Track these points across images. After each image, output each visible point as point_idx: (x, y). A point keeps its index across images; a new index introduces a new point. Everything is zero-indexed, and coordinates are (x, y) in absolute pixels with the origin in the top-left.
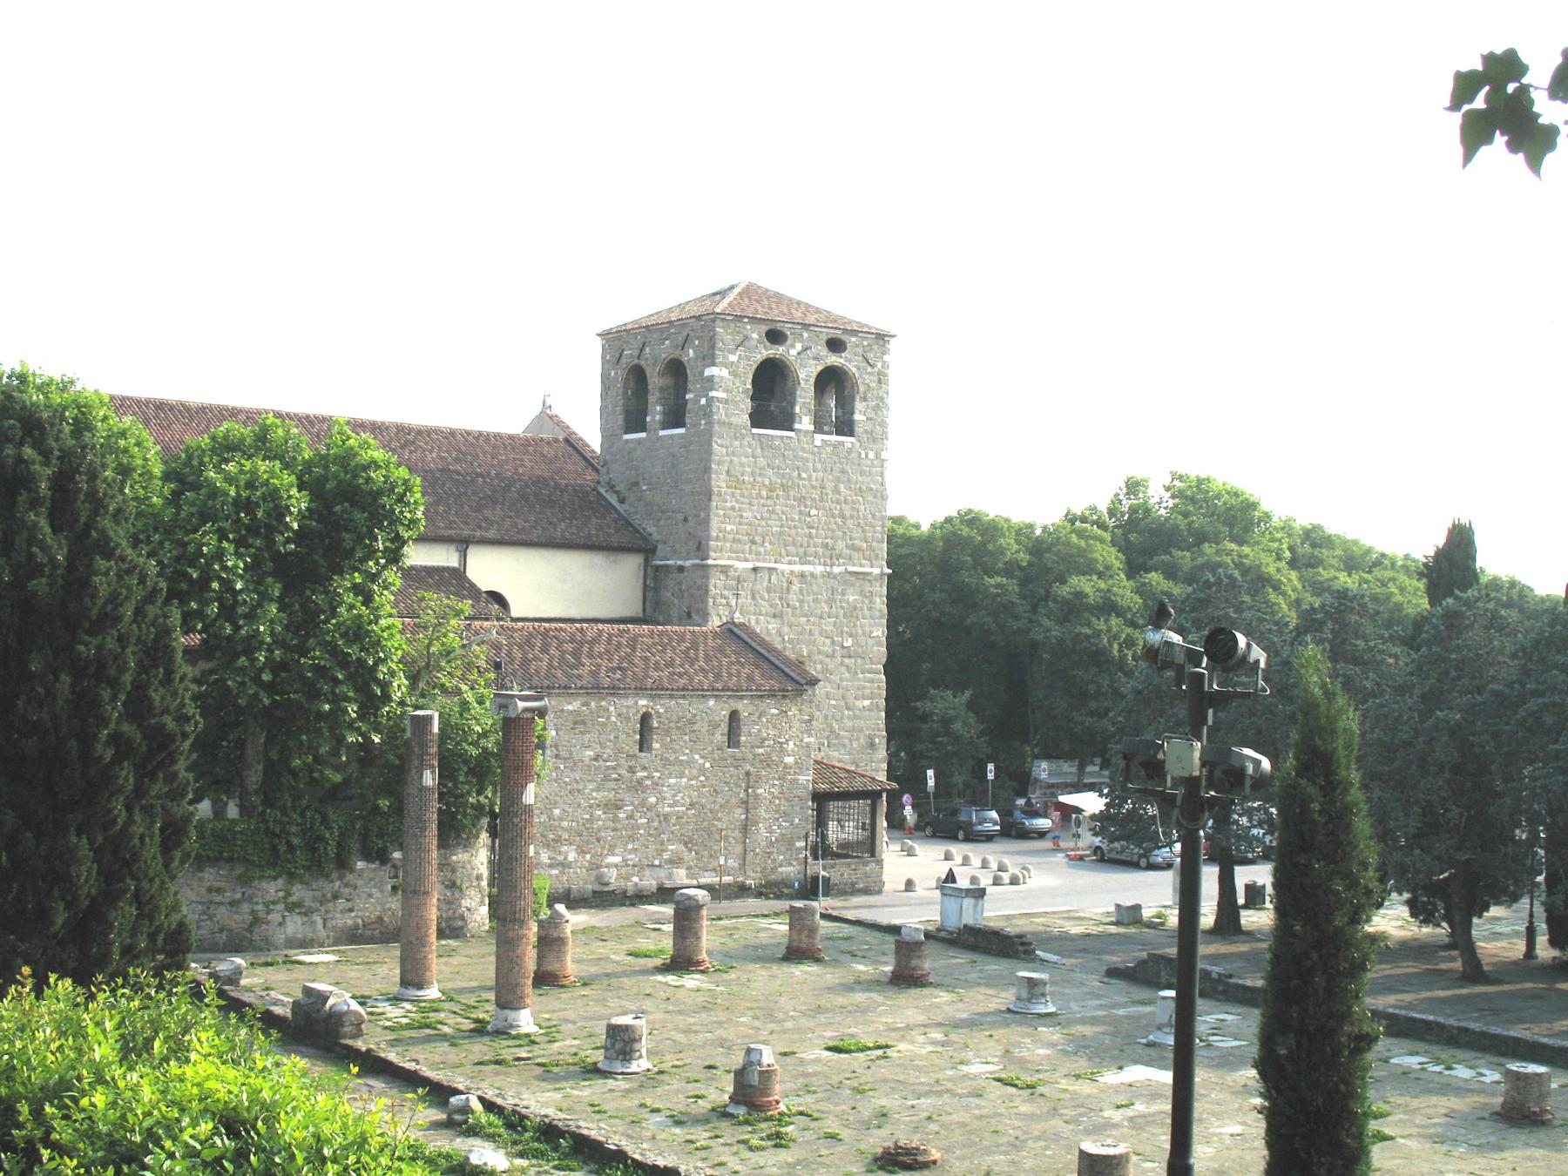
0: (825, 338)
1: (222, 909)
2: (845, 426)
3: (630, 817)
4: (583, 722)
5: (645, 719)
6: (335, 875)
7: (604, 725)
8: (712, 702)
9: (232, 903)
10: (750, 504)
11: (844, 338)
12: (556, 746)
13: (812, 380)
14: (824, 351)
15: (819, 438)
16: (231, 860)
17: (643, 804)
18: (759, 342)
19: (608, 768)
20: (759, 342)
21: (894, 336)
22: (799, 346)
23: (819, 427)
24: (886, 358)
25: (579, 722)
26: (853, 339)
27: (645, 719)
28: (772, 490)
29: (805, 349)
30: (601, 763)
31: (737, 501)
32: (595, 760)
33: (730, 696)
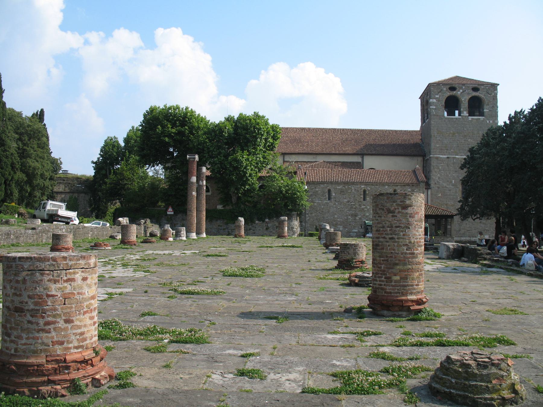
0: (471, 88)
1: (221, 230)
2: (482, 114)
3: (360, 219)
4: (343, 192)
5: (365, 191)
6: (250, 224)
7: (350, 192)
8: (386, 187)
9: (224, 229)
10: (446, 138)
11: (479, 87)
12: (335, 198)
13: (467, 101)
14: (471, 91)
15: (470, 118)
16: (223, 219)
17: (364, 215)
18: (446, 91)
19: (352, 205)
20: (446, 91)
21: (499, 85)
22: (461, 91)
23: (471, 114)
24: (495, 92)
25: (342, 192)
26: (482, 87)
27: (365, 191)
28: (454, 134)
29: (463, 92)
30: (350, 203)
31: (441, 138)
32: (348, 202)
33: (393, 185)
